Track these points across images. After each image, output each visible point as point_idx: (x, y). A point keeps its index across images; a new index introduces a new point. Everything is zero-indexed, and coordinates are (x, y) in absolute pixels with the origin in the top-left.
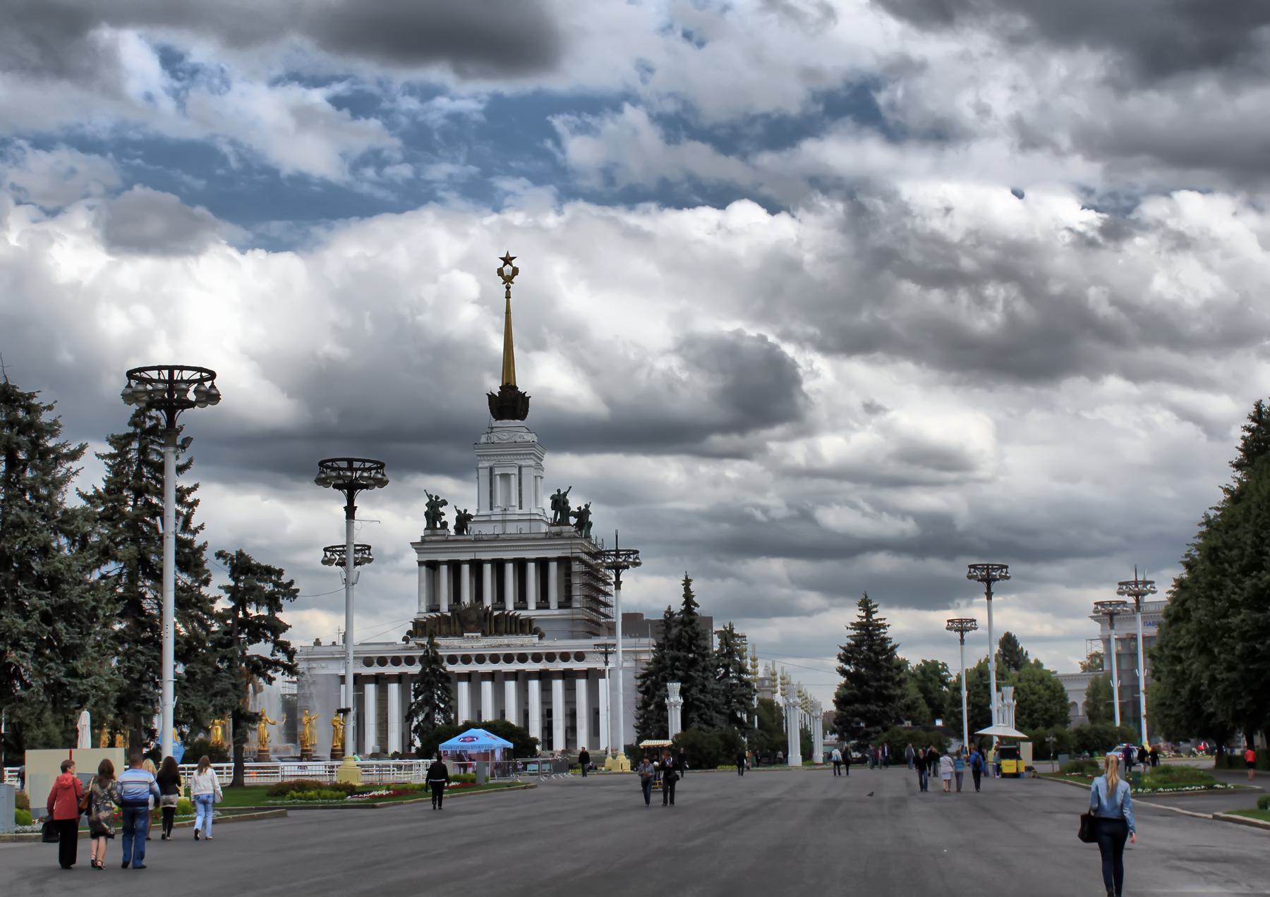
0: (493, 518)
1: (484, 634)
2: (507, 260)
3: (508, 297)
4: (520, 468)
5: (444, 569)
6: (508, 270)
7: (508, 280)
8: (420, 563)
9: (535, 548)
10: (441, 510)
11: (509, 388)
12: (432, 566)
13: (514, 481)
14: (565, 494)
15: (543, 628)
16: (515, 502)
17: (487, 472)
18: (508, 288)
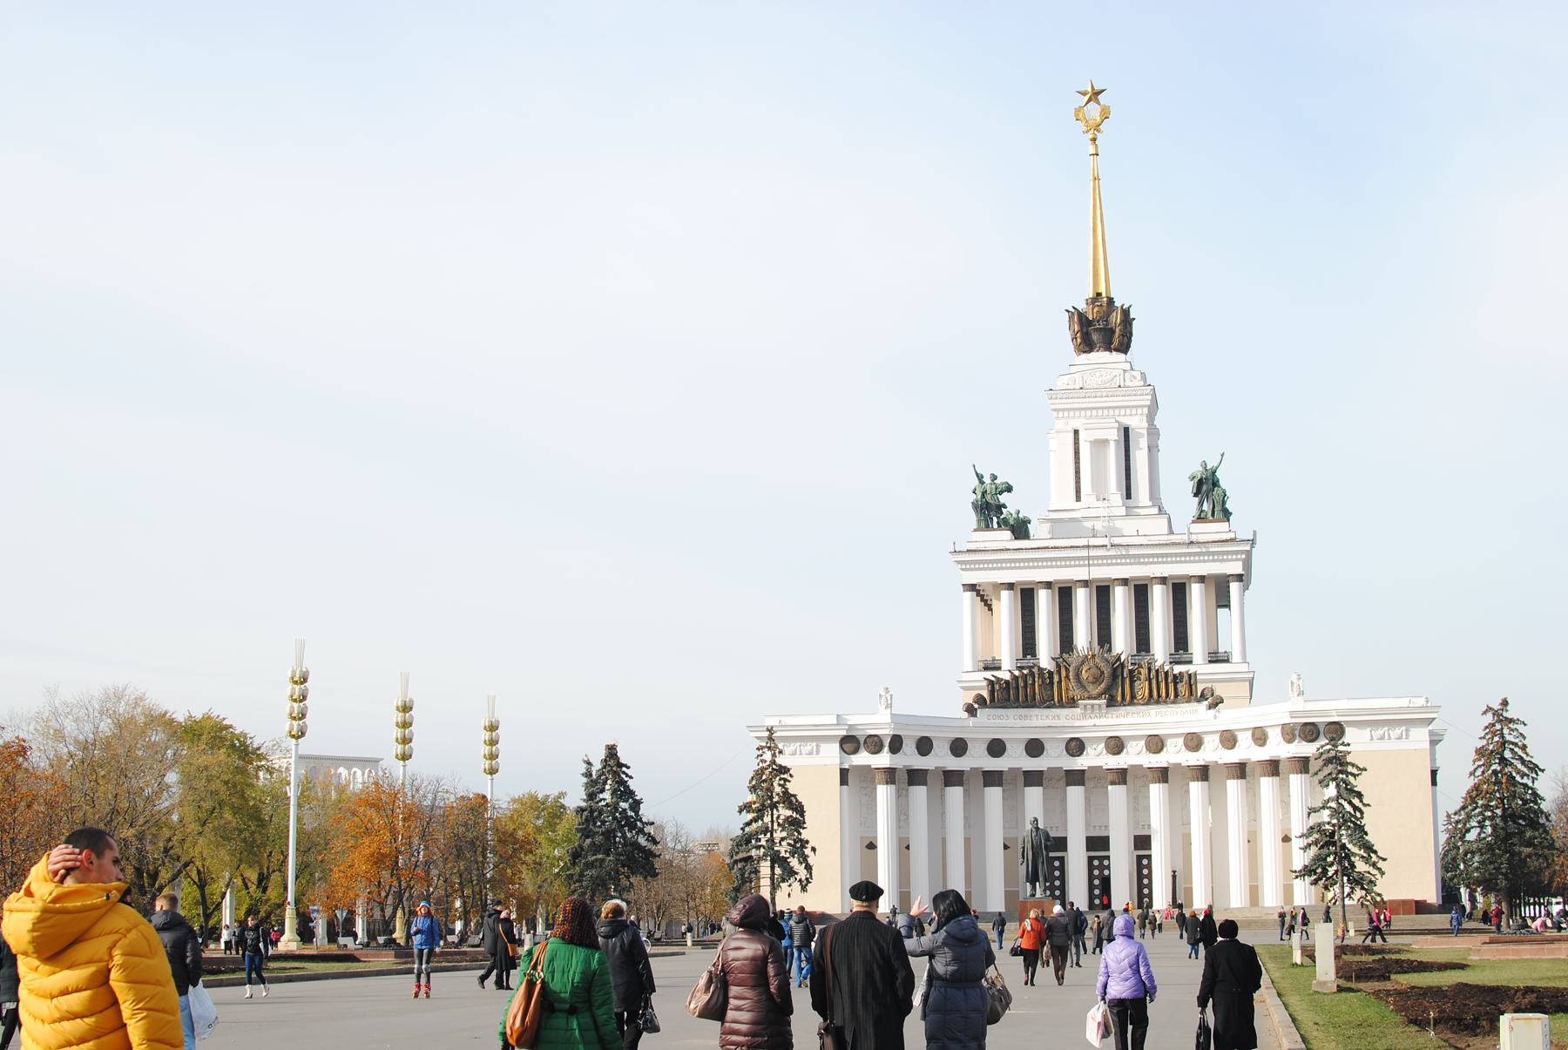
1: (1112, 703)
6: (1093, 111)
10: (1003, 498)
15: (1220, 690)
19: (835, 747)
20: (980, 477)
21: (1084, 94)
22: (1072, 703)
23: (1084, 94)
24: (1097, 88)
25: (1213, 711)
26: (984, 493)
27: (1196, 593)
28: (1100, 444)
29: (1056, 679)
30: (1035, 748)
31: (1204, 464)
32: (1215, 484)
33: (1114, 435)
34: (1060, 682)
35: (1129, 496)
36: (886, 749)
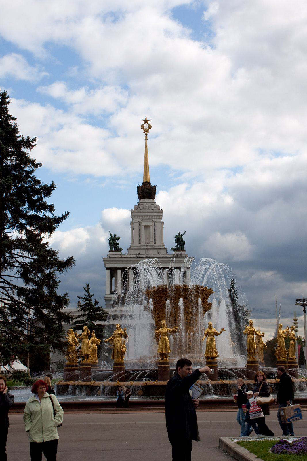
0: (141, 248)
2: (146, 121)
3: (146, 139)
4: (155, 223)
5: (119, 272)
6: (146, 126)
7: (146, 131)
8: (107, 269)
10: (117, 242)
11: (146, 183)
12: (113, 272)
13: (151, 229)
14: (182, 235)
16: (152, 240)
17: (138, 224)
18: (146, 135)
20: (111, 235)
24: (148, 119)
26: (113, 240)
28: (147, 227)
31: (179, 233)
32: (182, 240)
33: (151, 224)
35: (155, 243)
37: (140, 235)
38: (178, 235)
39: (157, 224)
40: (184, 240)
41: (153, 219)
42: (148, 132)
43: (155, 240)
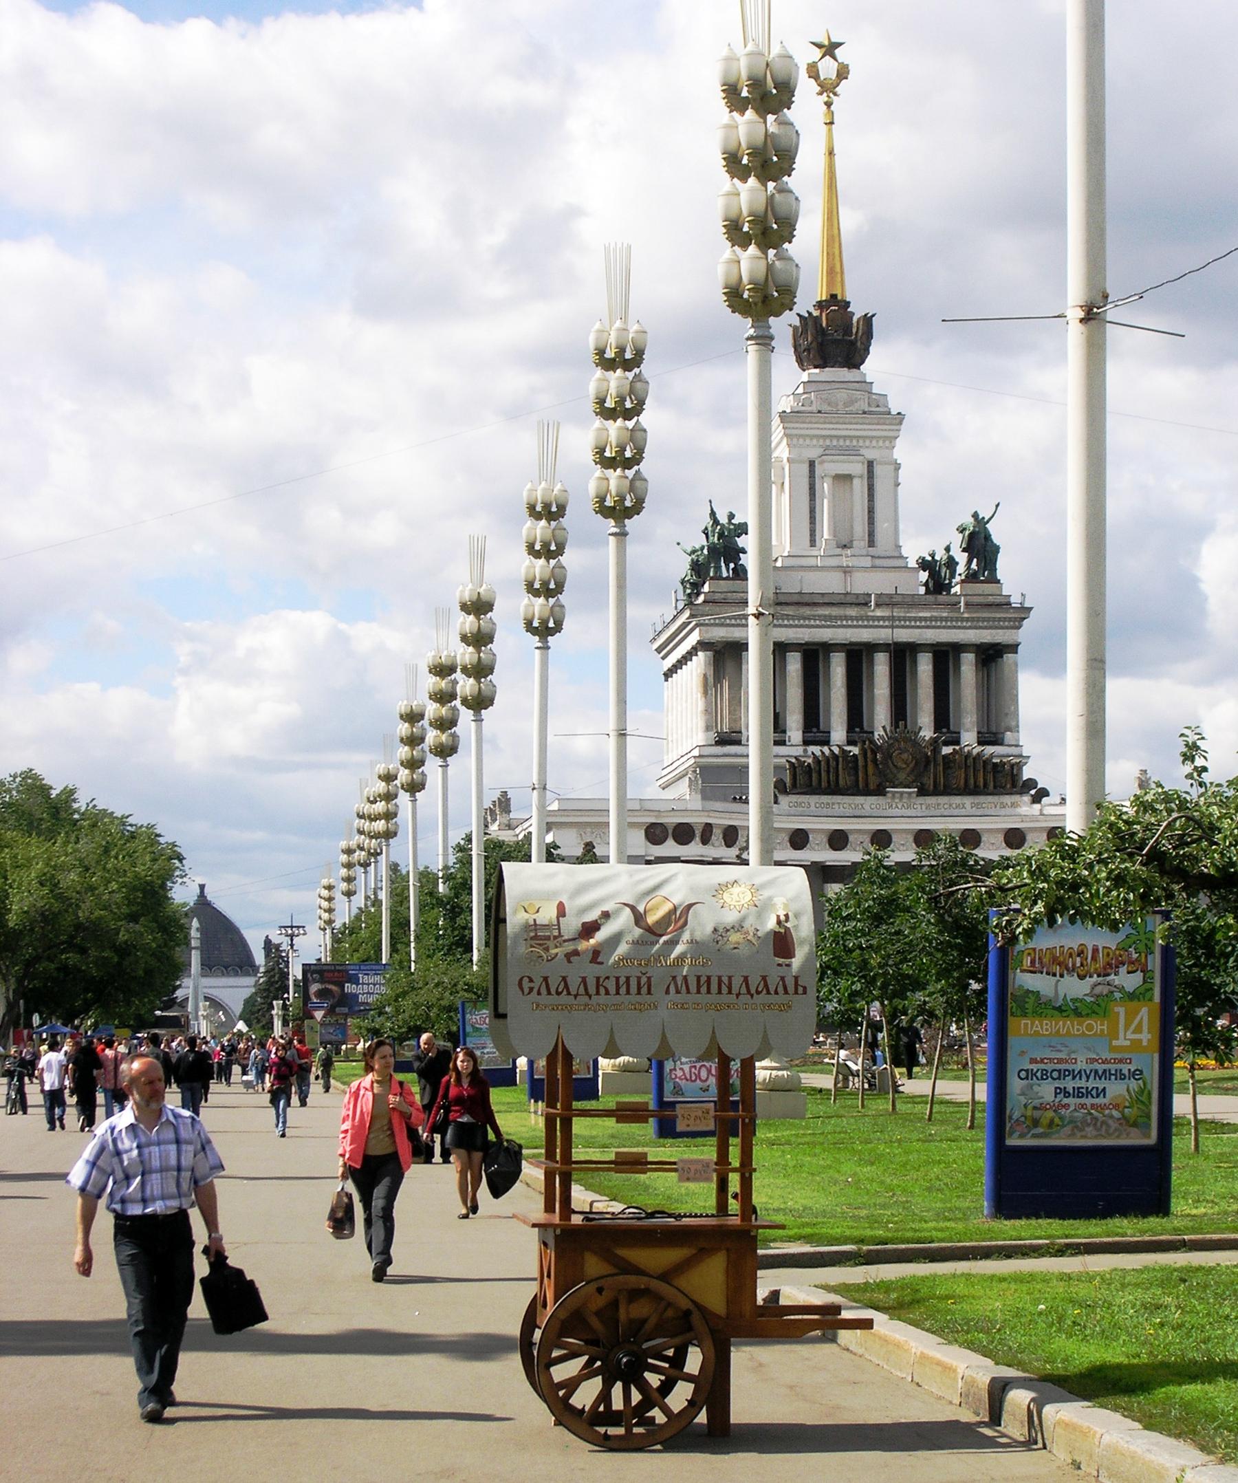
1: (922, 792)
2: (830, 49)
4: (870, 464)
6: (828, 68)
9: (930, 623)
13: (859, 486)
16: (860, 528)
17: (806, 467)
18: (828, 104)
19: (641, 834)
21: (819, 46)
22: (880, 791)
23: (819, 46)
25: (1037, 806)
26: (721, 535)
27: (968, 661)
28: (843, 479)
29: (861, 763)
30: (838, 840)
32: (988, 537)
33: (858, 468)
34: (866, 766)
35: (871, 543)
36: (698, 839)
37: (812, 511)
38: (972, 520)
39: (878, 470)
40: (996, 539)
41: (862, 451)
42: (835, 94)
43: (871, 534)
